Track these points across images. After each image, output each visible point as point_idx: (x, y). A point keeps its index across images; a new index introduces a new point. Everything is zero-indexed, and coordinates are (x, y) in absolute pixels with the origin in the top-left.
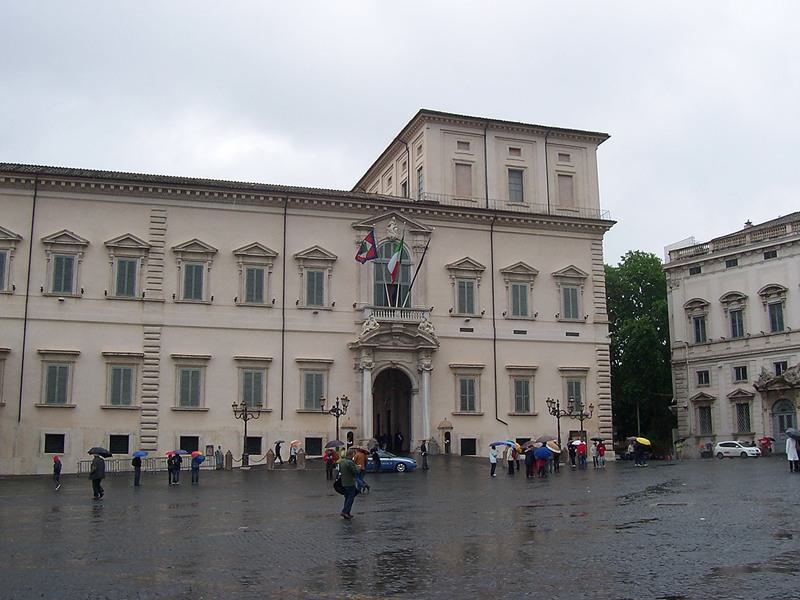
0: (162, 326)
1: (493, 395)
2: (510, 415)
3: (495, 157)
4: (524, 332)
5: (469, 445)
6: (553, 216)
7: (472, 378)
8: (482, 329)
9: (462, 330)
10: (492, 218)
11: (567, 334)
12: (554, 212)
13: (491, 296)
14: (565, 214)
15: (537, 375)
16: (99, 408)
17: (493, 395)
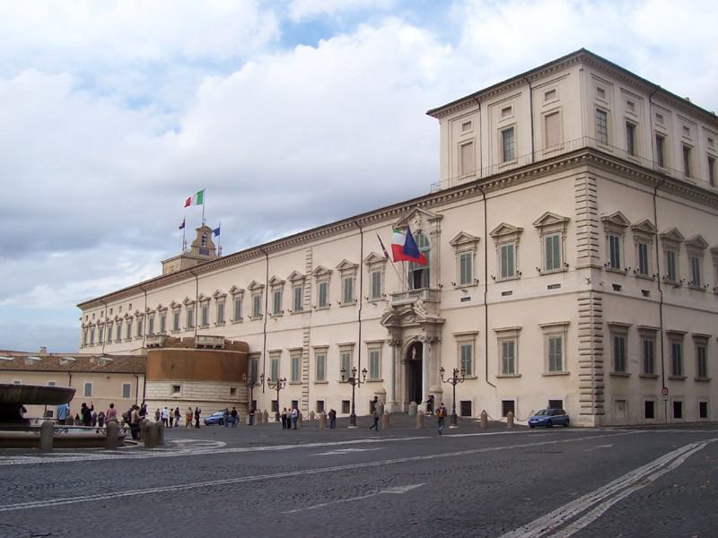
0: (309, 328)
1: (488, 356)
2: (498, 377)
3: (487, 123)
4: (510, 293)
5: (466, 406)
6: (537, 163)
7: (469, 343)
8: (476, 295)
9: (462, 300)
10: (481, 187)
11: (550, 287)
12: (539, 158)
13: (487, 260)
14: (553, 155)
15: (522, 334)
16: (540, 376)
17: (488, 356)
